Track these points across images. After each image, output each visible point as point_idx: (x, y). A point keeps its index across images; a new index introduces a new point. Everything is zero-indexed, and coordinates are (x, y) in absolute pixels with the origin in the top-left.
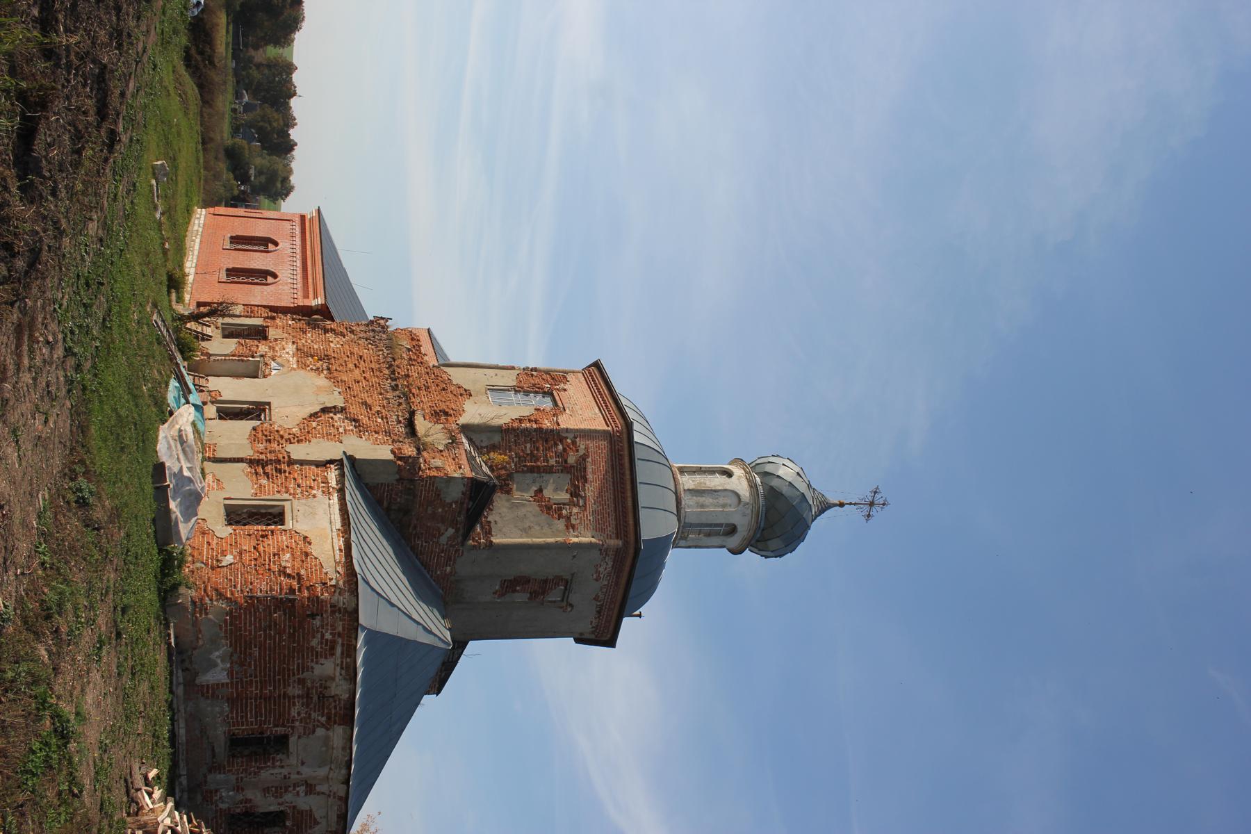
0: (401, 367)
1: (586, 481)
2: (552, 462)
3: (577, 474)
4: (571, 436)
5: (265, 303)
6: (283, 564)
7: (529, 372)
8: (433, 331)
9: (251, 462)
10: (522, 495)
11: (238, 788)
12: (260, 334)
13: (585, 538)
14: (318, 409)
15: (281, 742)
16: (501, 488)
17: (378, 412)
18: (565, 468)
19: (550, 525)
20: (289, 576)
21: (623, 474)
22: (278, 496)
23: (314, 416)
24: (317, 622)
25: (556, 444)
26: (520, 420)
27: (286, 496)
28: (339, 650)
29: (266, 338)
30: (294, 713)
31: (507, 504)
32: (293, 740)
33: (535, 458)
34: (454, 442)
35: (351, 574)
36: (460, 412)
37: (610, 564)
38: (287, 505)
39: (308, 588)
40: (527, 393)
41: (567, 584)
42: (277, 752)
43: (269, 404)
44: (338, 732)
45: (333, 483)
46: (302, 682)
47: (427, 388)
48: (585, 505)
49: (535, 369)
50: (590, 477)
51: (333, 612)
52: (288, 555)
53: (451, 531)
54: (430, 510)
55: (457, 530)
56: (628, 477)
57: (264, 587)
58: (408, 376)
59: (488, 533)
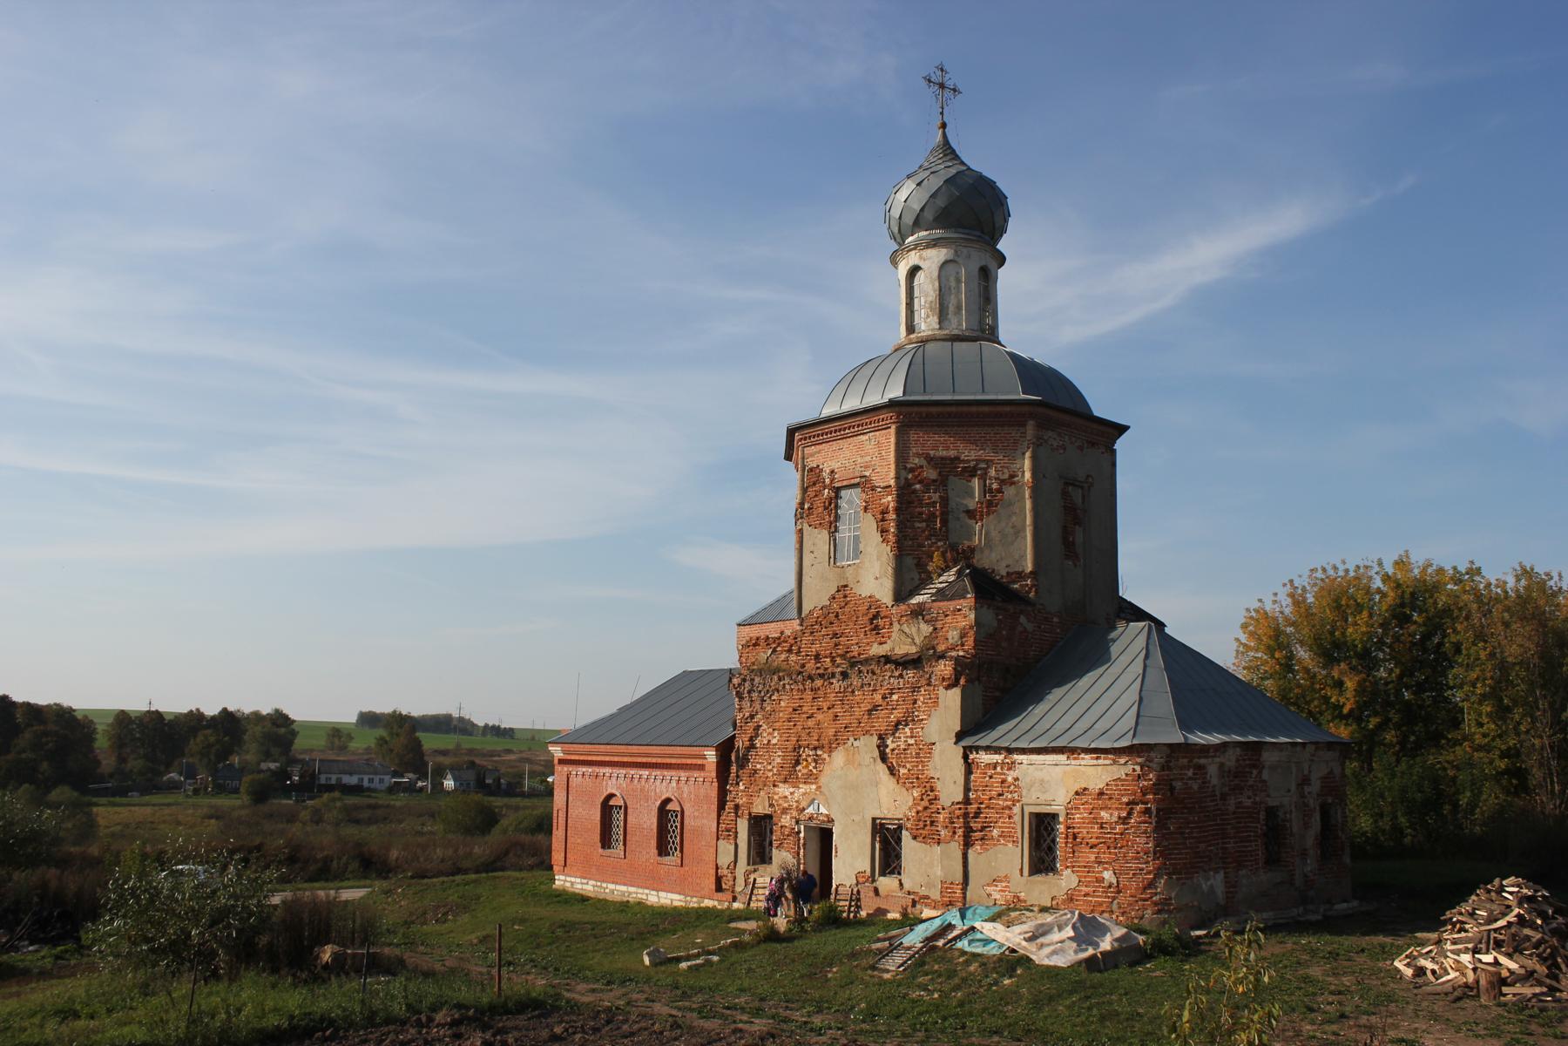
0: (802, 665)
1: (957, 458)
2: (935, 497)
3: (948, 468)
4: (903, 473)
5: (715, 815)
6: (1115, 819)
7: (803, 512)
8: (740, 619)
9: (967, 844)
10: (978, 533)
11: (1304, 854)
12: (761, 827)
13: (1026, 469)
14: (882, 768)
15: (1271, 812)
16: (967, 558)
17: (884, 698)
18: (942, 482)
19: (1010, 504)
20: (1130, 814)
21: (950, 414)
22: (1017, 818)
23: (892, 771)
24: (1178, 785)
25: (915, 491)
26: (883, 531)
27: (1017, 809)
28: (1202, 761)
29: (770, 817)
30: (1248, 803)
31: (986, 552)
32: (1272, 803)
33: (932, 516)
34: (919, 613)
35: (1130, 751)
36: (872, 602)
37: (1050, 433)
38: (1028, 810)
39: (1144, 794)
40: (837, 518)
41: (1070, 482)
42: (1281, 814)
43: (874, 819)
44: (1268, 757)
45: (998, 758)
46: (1224, 797)
47: (835, 635)
48: (987, 462)
49: (801, 504)
50: (952, 453)
51: (1169, 769)
52: (1103, 813)
53: (1023, 619)
54: (1004, 644)
55: (1021, 612)
56: (953, 409)
57: (1143, 840)
58: (817, 657)
59: (1020, 575)
